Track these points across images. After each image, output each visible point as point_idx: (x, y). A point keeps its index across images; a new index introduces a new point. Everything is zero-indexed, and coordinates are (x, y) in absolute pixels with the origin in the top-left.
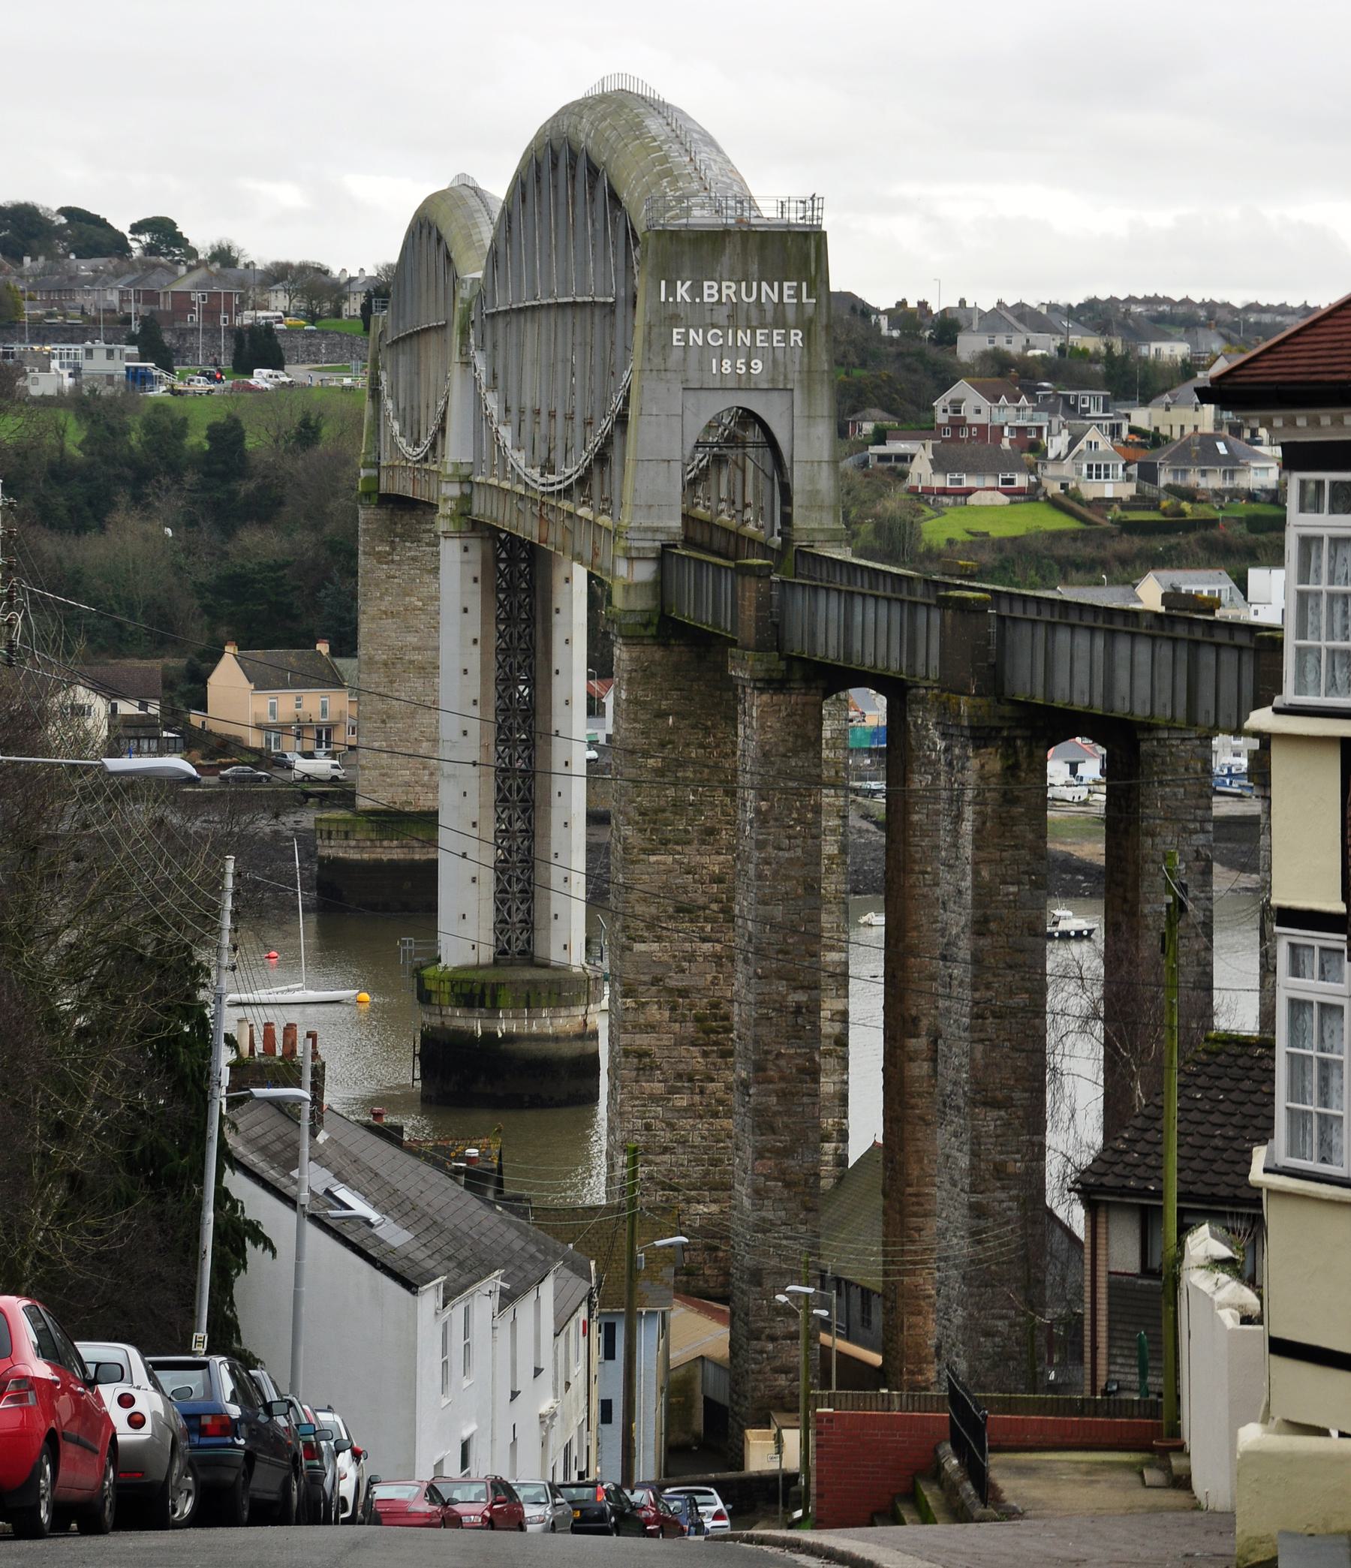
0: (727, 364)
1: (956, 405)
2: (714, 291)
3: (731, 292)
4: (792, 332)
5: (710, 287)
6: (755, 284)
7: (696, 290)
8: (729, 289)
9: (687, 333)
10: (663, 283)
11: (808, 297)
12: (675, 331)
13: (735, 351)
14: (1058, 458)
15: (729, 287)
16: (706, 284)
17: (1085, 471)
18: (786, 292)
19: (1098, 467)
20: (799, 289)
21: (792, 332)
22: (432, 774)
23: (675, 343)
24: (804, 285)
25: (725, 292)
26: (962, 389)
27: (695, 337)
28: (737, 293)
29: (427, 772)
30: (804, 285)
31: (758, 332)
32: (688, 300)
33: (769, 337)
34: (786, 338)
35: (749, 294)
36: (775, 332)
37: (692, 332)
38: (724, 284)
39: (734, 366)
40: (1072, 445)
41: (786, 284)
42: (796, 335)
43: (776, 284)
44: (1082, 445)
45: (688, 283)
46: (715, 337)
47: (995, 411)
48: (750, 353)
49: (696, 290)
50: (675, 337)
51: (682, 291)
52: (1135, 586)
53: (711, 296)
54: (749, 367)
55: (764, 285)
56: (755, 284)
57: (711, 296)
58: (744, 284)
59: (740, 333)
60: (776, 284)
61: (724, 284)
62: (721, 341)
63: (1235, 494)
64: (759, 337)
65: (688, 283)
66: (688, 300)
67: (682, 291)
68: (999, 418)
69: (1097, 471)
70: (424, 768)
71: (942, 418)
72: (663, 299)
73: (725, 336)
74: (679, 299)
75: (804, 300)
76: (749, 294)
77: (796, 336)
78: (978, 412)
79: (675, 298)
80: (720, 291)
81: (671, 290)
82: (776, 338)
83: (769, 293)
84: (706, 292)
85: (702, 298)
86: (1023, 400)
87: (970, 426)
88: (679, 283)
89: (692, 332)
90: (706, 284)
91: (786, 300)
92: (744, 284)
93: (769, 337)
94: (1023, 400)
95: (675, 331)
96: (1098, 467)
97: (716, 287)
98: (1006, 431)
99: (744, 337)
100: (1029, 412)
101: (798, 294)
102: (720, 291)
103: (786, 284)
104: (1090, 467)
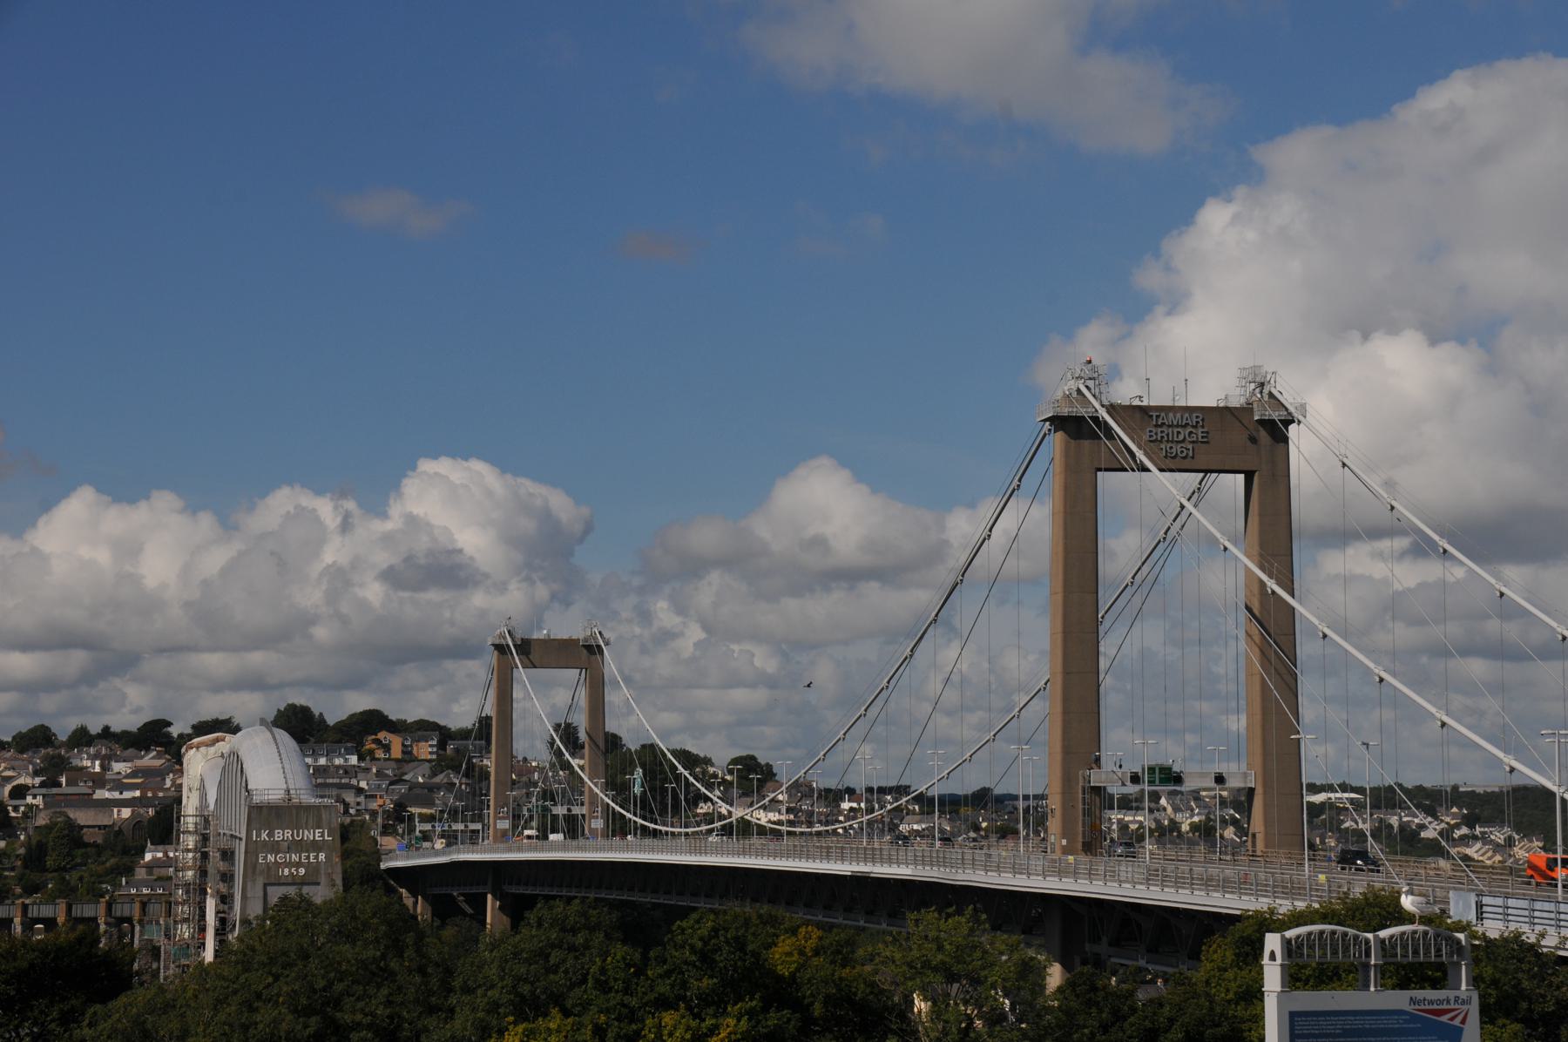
3: (289, 835)
7: (271, 835)
8: (288, 834)
9: (267, 856)
13: (289, 864)
16: (277, 831)
18: (317, 835)
20: (323, 832)
23: (260, 861)
25: (286, 835)
27: (271, 858)
28: (292, 835)
32: (267, 839)
34: (316, 857)
35: (298, 836)
37: (269, 856)
38: (286, 831)
45: (267, 832)
48: (298, 865)
49: (271, 835)
51: (264, 836)
53: (279, 837)
55: (306, 832)
57: (279, 837)
58: (295, 831)
61: (286, 831)
65: (267, 832)
66: (267, 839)
73: (285, 857)
75: (326, 838)
76: (298, 836)
77: (322, 856)
80: (283, 834)
83: (308, 835)
89: (269, 856)
91: (317, 838)
92: (295, 831)
93: (308, 858)
97: (282, 833)
99: (295, 858)
101: (323, 836)
102: (283, 834)
103: (317, 831)
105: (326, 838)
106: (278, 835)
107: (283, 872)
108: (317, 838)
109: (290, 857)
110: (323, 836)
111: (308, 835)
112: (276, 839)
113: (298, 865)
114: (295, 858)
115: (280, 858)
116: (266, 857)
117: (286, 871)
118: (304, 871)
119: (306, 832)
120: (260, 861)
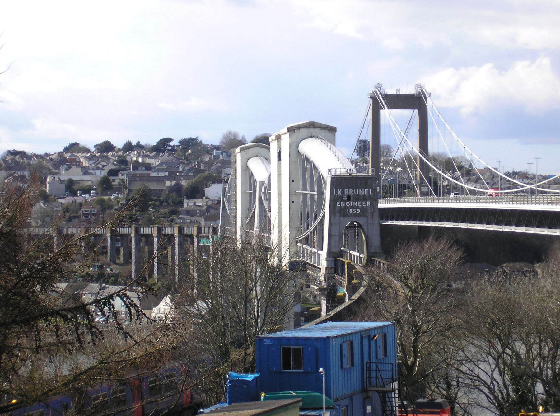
0: (351, 210)
3: (352, 192)
7: (343, 192)
13: (352, 207)
18: (366, 192)
27: (343, 204)
28: (353, 192)
34: (366, 204)
35: (356, 193)
38: (350, 190)
46: (348, 204)
48: (357, 207)
50: (338, 204)
54: (356, 210)
55: (360, 190)
57: (347, 193)
61: (350, 190)
75: (370, 194)
76: (356, 193)
77: (368, 203)
80: (349, 192)
81: (336, 192)
82: (363, 204)
83: (361, 192)
91: (366, 194)
93: (362, 204)
99: (355, 204)
101: (369, 192)
102: (349, 192)
103: (366, 190)
105: (370, 194)
110: (369, 192)
111: (361, 192)
113: (357, 207)
115: (348, 204)
116: (340, 204)
117: (351, 211)
119: (360, 190)
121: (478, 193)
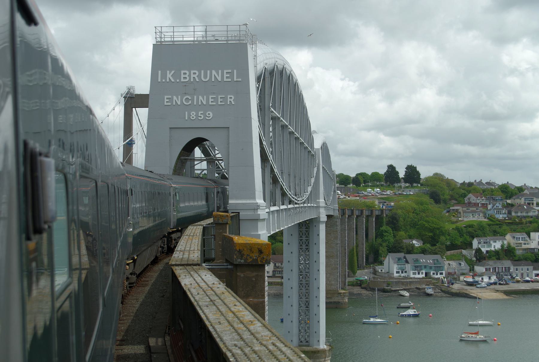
1: (469, 199)
2: (186, 76)
3: (195, 76)
4: (229, 96)
5: (185, 74)
6: (208, 72)
8: (194, 75)
10: (160, 72)
11: (237, 79)
12: (166, 97)
14: (490, 210)
15: (195, 73)
16: (183, 72)
17: (496, 212)
18: (225, 75)
19: (499, 211)
20: (232, 74)
21: (229, 96)
22: (330, 282)
24: (235, 71)
25: (192, 76)
26: (470, 195)
28: (200, 76)
29: (329, 281)
30: (235, 71)
31: (210, 97)
33: (216, 99)
34: (225, 99)
35: (205, 77)
36: (219, 97)
37: (175, 98)
38: (192, 72)
39: (197, 115)
40: (493, 207)
41: (225, 71)
42: (231, 98)
43: (220, 71)
44: (495, 207)
47: (477, 200)
48: (205, 107)
50: (166, 100)
51: (169, 75)
52: (505, 236)
53: (185, 78)
55: (214, 72)
56: (208, 72)
57: (185, 78)
58: (202, 72)
59: (200, 98)
60: (220, 71)
61: (192, 72)
62: (190, 102)
63: (528, 217)
64: (211, 100)
65: (173, 72)
66: (173, 80)
67: (169, 75)
68: (478, 202)
69: (499, 212)
70: (328, 280)
71: (466, 202)
72: (159, 80)
73: (193, 100)
74: (168, 80)
76: (205, 77)
77: (231, 99)
78: (474, 200)
79: (166, 80)
80: (190, 76)
81: (164, 76)
82: (219, 100)
84: (183, 76)
85: (180, 79)
86: (483, 198)
87: (472, 203)
88: (168, 72)
89: (175, 98)
90: (183, 72)
92: (202, 72)
93: (216, 99)
94: (483, 198)
95: (166, 97)
96: (499, 211)
98: (480, 204)
99: (202, 100)
100: (485, 200)
102: (190, 76)
104: (497, 211)
106: (186, 76)
107: (189, 115)
108: (225, 80)
109: (198, 99)
112: (182, 80)
114: (202, 100)
116: (171, 100)
117: (193, 114)
118: (211, 115)
119: (214, 72)
120: (166, 104)
121: (490, 258)
